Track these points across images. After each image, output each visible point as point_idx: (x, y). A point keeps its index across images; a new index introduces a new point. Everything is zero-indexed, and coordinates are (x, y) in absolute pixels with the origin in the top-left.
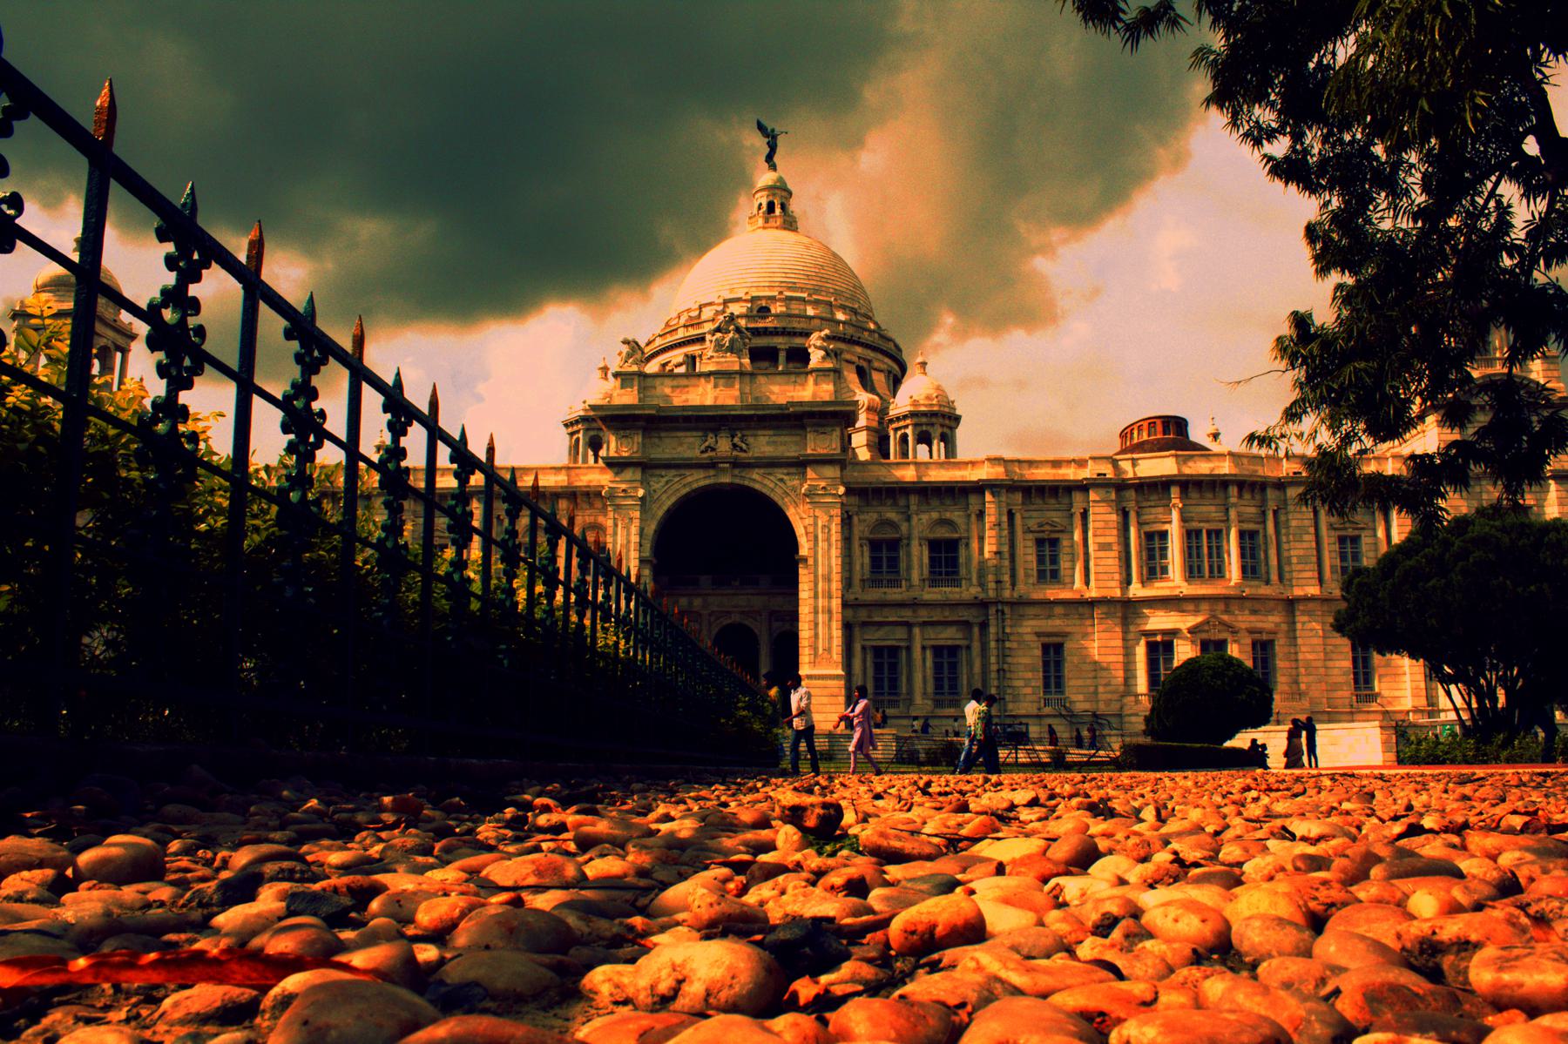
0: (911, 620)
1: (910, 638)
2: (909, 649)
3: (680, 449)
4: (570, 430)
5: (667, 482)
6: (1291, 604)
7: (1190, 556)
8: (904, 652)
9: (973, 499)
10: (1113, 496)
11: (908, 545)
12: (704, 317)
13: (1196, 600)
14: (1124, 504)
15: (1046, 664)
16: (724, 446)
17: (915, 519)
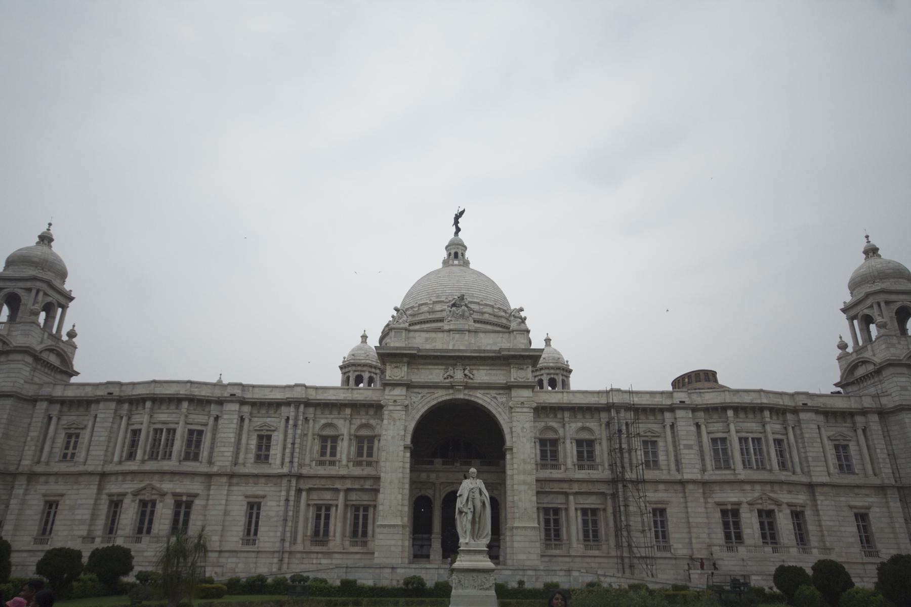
0: (568, 491)
1: (567, 502)
2: (567, 510)
3: (430, 377)
4: (344, 371)
5: (422, 397)
6: (811, 487)
7: (742, 454)
8: (564, 512)
9: (604, 416)
10: (690, 415)
11: (564, 443)
12: (420, 311)
13: (752, 482)
14: (697, 421)
15: (655, 522)
16: (459, 375)
17: (567, 426)
